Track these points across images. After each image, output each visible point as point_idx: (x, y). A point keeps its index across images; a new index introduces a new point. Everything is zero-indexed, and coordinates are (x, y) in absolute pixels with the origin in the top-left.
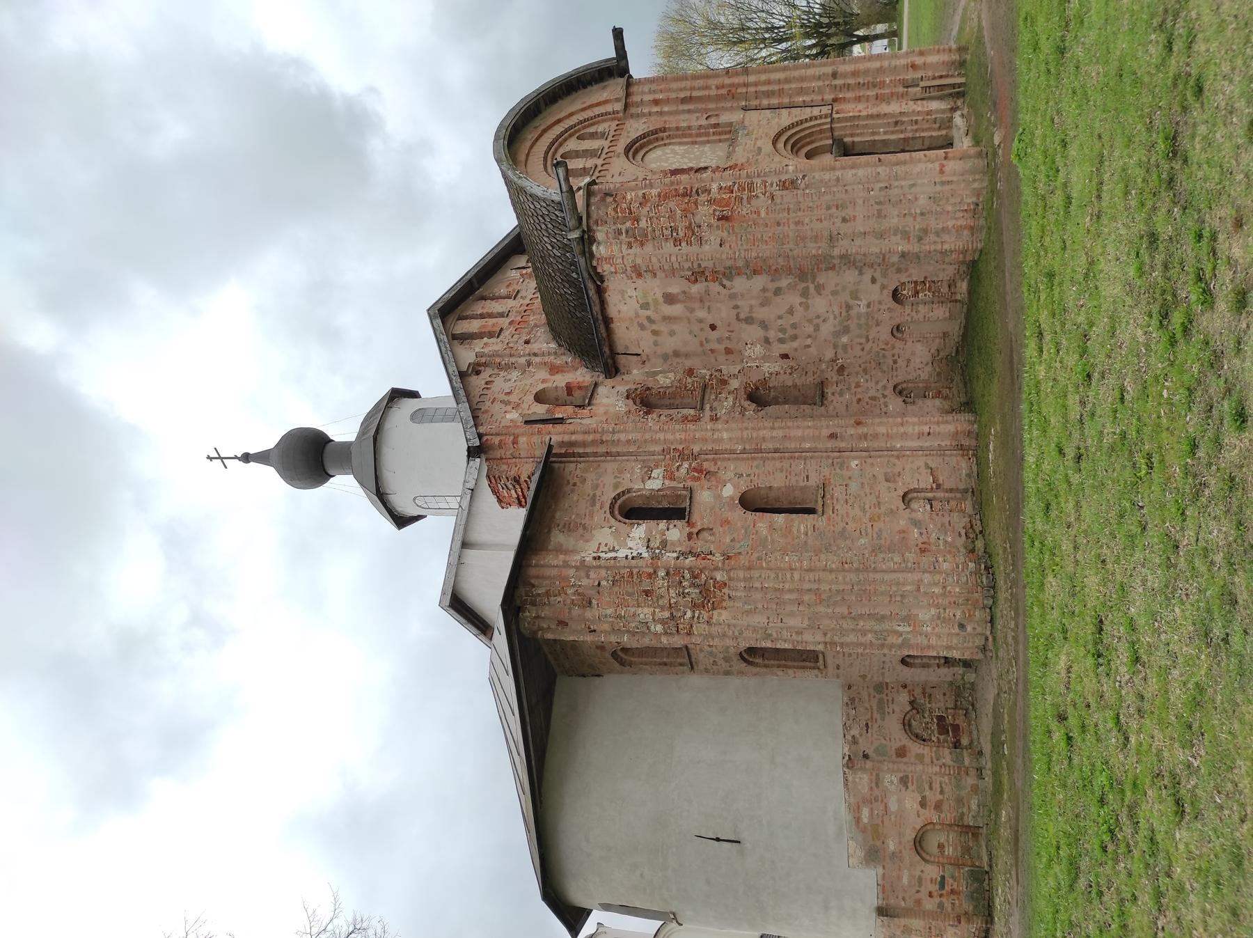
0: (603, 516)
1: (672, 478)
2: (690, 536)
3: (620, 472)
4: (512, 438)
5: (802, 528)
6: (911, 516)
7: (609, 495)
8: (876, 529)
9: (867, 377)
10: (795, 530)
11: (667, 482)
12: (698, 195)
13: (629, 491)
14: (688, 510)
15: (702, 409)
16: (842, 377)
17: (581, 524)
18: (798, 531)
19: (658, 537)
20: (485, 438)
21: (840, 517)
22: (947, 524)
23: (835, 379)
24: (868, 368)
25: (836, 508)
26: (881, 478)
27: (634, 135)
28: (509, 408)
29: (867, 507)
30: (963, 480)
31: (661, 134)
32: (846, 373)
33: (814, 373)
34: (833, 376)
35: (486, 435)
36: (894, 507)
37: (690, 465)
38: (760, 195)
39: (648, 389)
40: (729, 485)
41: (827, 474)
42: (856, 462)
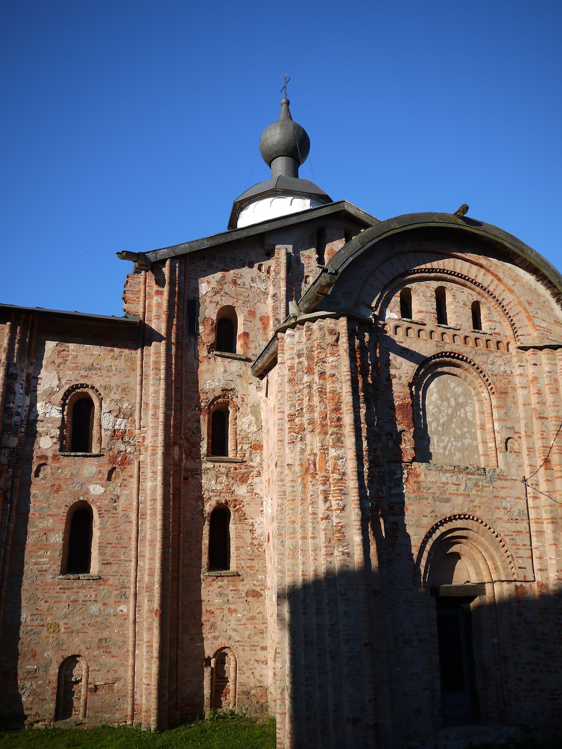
0: (73, 379)
3: (123, 390)
5: (44, 560)
6: (54, 661)
7: (97, 381)
8: (38, 629)
9: (244, 621)
10: (41, 553)
12: (331, 435)
14: (88, 454)
16: (244, 594)
18: (41, 557)
19: (45, 429)
21: (56, 595)
22: (41, 697)
23: (241, 588)
24: (256, 621)
25: (67, 591)
26: (106, 634)
29: (65, 621)
30: (97, 714)
32: (250, 599)
33: (251, 568)
34: (244, 587)
36: (64, 647)
38: (328, 504)
40: (102, 490)
41: (110, 582)
42: (125, 610)
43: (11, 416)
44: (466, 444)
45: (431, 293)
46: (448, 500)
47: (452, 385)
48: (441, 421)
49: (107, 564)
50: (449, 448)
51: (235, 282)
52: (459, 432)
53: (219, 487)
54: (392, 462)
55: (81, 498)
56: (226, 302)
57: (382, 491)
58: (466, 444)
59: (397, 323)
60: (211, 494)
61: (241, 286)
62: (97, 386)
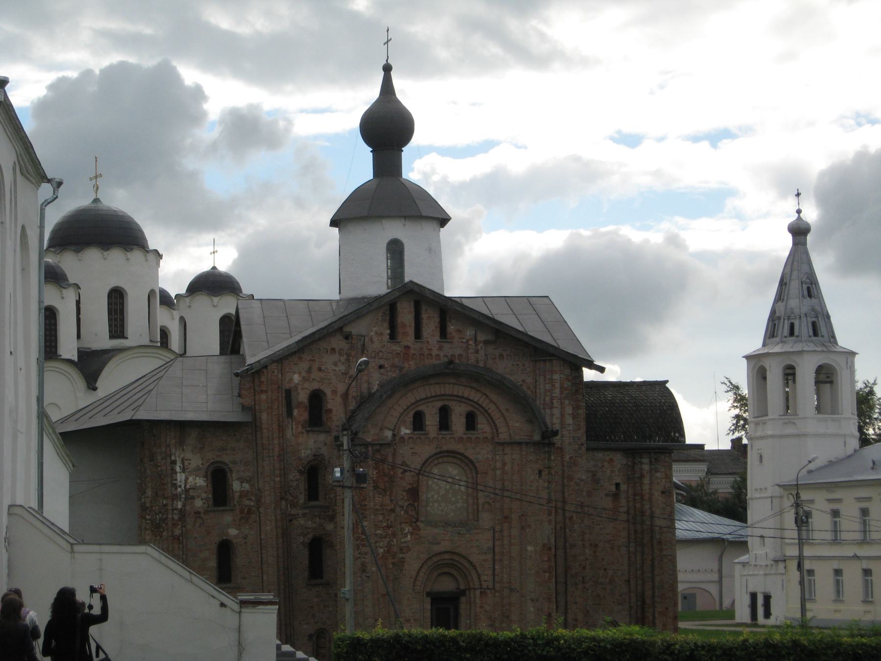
1: (240, 497)
2: (198, 513)
4: (265, 389)
7: (226, 458)
11: (238, 494)
13: (231, 471)
15: (304, 508)
17: (204, 445)
20: (265, 371)
27: (470, 453)
28: (304, 374)
31: (474, 472)
35: (267, 371)
37: (253, 506)
38: (359, 551)
39: (326, 469)
43: (176, 489)
44: (459, 506)
45: (435, 410)
46: (439, 544)
47: (451, 470)
48: (441, 494)
49: (244, 578)
50: (446, 509)
51: (320, 370)
52: (453, 499)
53: (314, 525)
54: (403, 523)
55: (224, 538)
56: (315, 386)
57: (393, 541)
58: (459, 506)
59: (410, 436)
60: (309, 530)
61: (326, 371)
62: (226, 461)
